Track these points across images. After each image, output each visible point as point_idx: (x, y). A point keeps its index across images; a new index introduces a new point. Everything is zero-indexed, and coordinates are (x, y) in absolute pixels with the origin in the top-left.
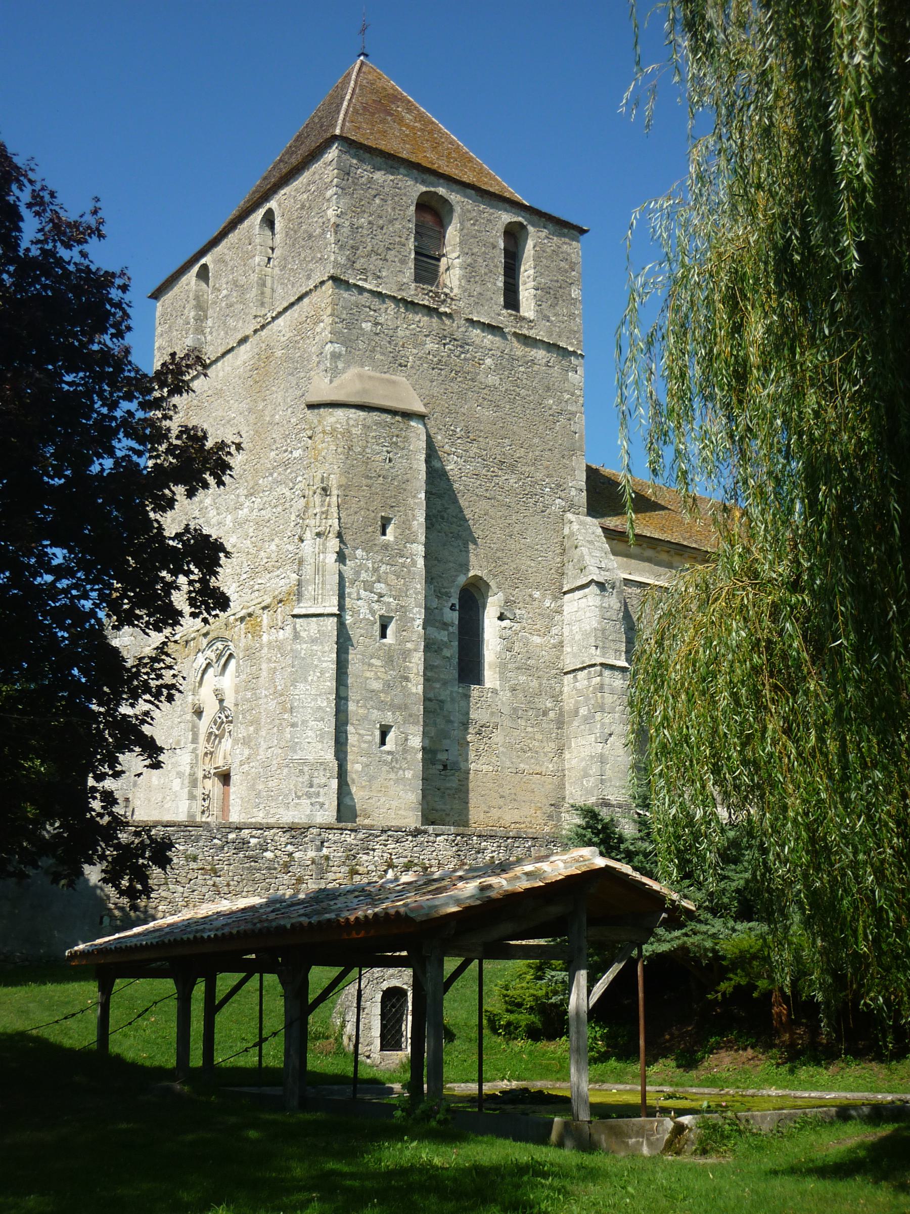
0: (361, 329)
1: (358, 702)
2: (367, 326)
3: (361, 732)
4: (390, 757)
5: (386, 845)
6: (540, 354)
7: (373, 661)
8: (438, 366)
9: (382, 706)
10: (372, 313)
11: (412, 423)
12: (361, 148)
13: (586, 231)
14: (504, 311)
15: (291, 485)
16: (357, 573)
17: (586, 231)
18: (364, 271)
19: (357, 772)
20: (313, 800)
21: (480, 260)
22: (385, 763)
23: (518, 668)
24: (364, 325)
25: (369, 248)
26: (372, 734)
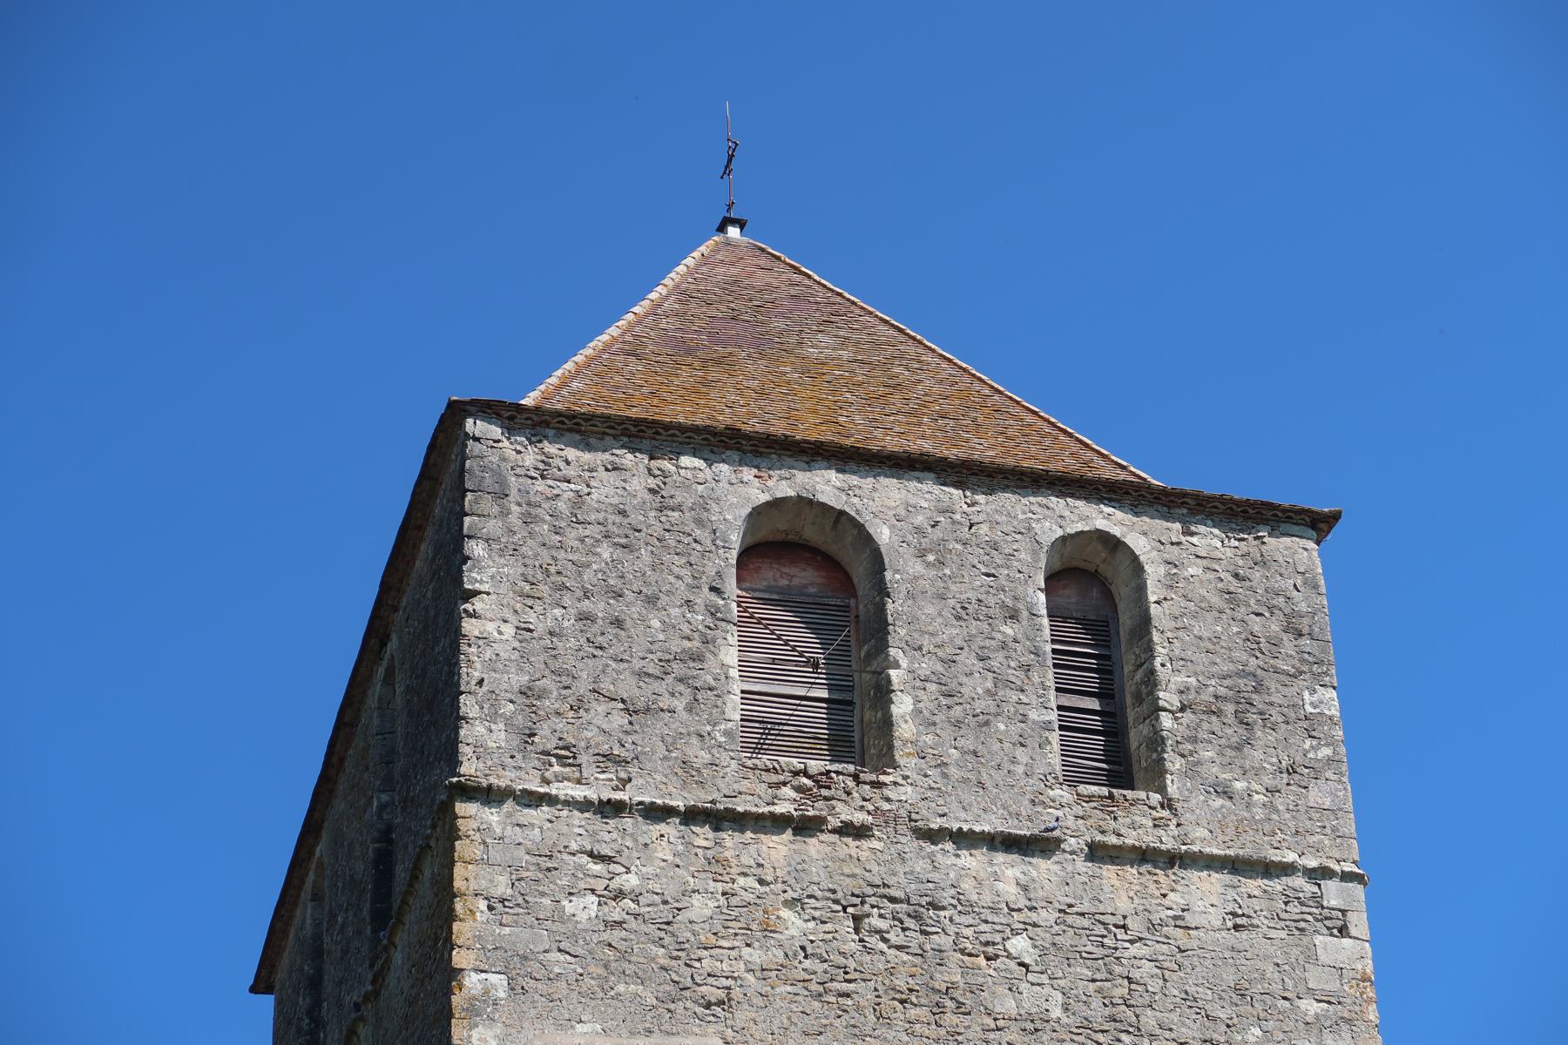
0: (563, 919)
2: (584, 908)
6: (1205, 894)
8: (833, 986)
10: (597, 868)
12: (547, 424)
13: (1334, 517)
14: (1062, 794)
17: (1334, 517)
18: (566, 755)
21: (968, 660)
24: (569, 907)
25: (582, 687)
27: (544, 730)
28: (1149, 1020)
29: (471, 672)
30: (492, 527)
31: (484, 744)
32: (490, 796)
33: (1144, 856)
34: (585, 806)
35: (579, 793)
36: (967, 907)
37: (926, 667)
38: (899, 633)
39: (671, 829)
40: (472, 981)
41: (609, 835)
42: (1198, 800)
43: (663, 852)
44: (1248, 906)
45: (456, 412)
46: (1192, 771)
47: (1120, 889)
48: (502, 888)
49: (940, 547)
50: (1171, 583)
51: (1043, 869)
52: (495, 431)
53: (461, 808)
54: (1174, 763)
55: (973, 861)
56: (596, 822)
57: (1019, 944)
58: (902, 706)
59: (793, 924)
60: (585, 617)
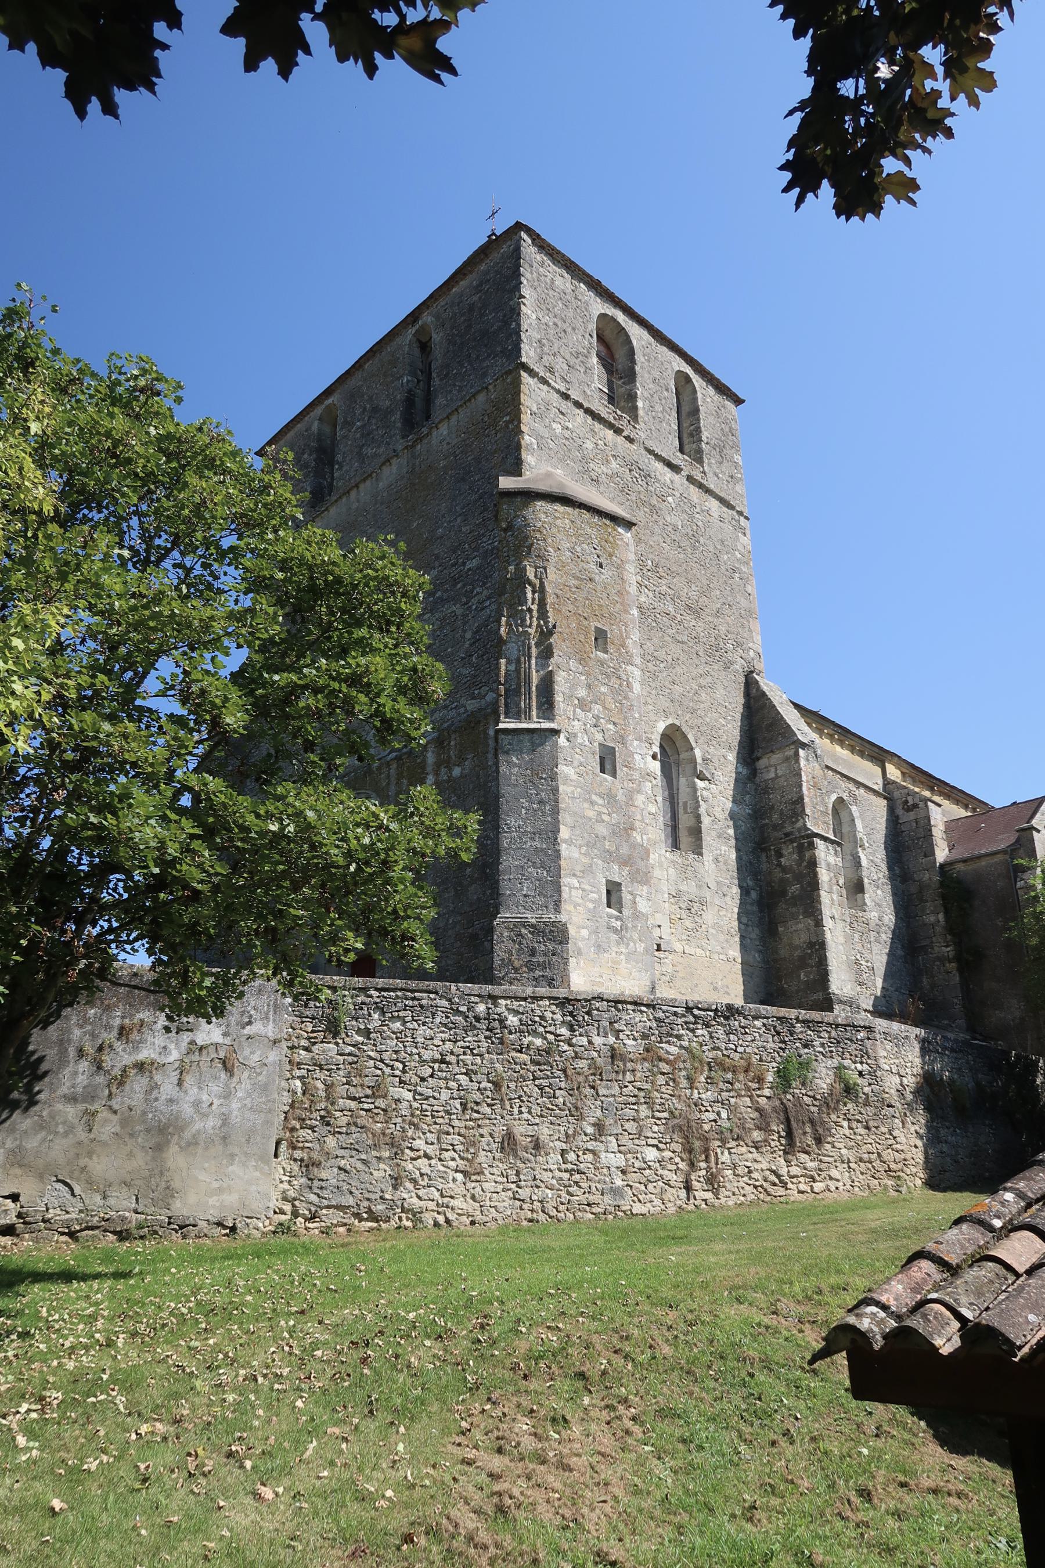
1: (581, 846)
3: (587, 887)
4: (619, 923)
5: (693, 1031)
7: (594, 797)
9: (609, 857)
11: (620, 530)
13: (743, 401)
15: (464, 600)
16: (574, 687)
17: (743, 401)
19: (583, 939)
20: (538, 973)
22: (615, 931)
23: (719, 836)
26: (599, 892)
27: (545, 358)
28: (702, 540)
29: (524, 326)
30: (528, 275)
31: (528, 354)
32: (532, 373)
33: (701, 486)
34: (558, 391)
35: (557, 386)
36: (658, 481)
37: (646, 394)
38: (639, 379)
39: (581, 412)
40: (526, 437)
41: (566, 406)
42: (713, 473)
43: (579, 420)
44: (725, 516)
45: (518, 226)
46: (709, 464)
47: (694, 492)
48: (534, 409)
49: (649, 355)
50: (704, 401)
51: (676, 477)
52: (529, 241)
53: (522, 373)
54: (706, 460)
55: (659, 466)
56: (561, 400)
57: (670, 499)
58: (640, 404)
59: (614, 464)
60: (555, 324)
